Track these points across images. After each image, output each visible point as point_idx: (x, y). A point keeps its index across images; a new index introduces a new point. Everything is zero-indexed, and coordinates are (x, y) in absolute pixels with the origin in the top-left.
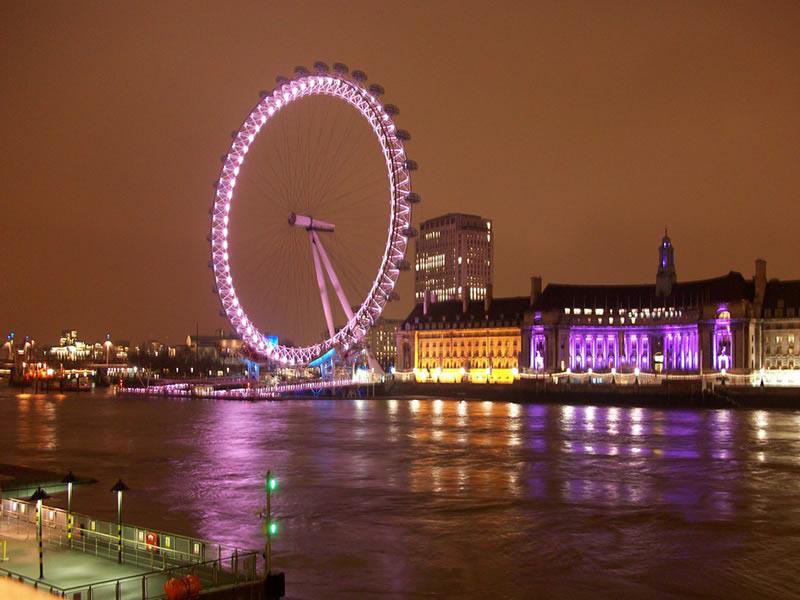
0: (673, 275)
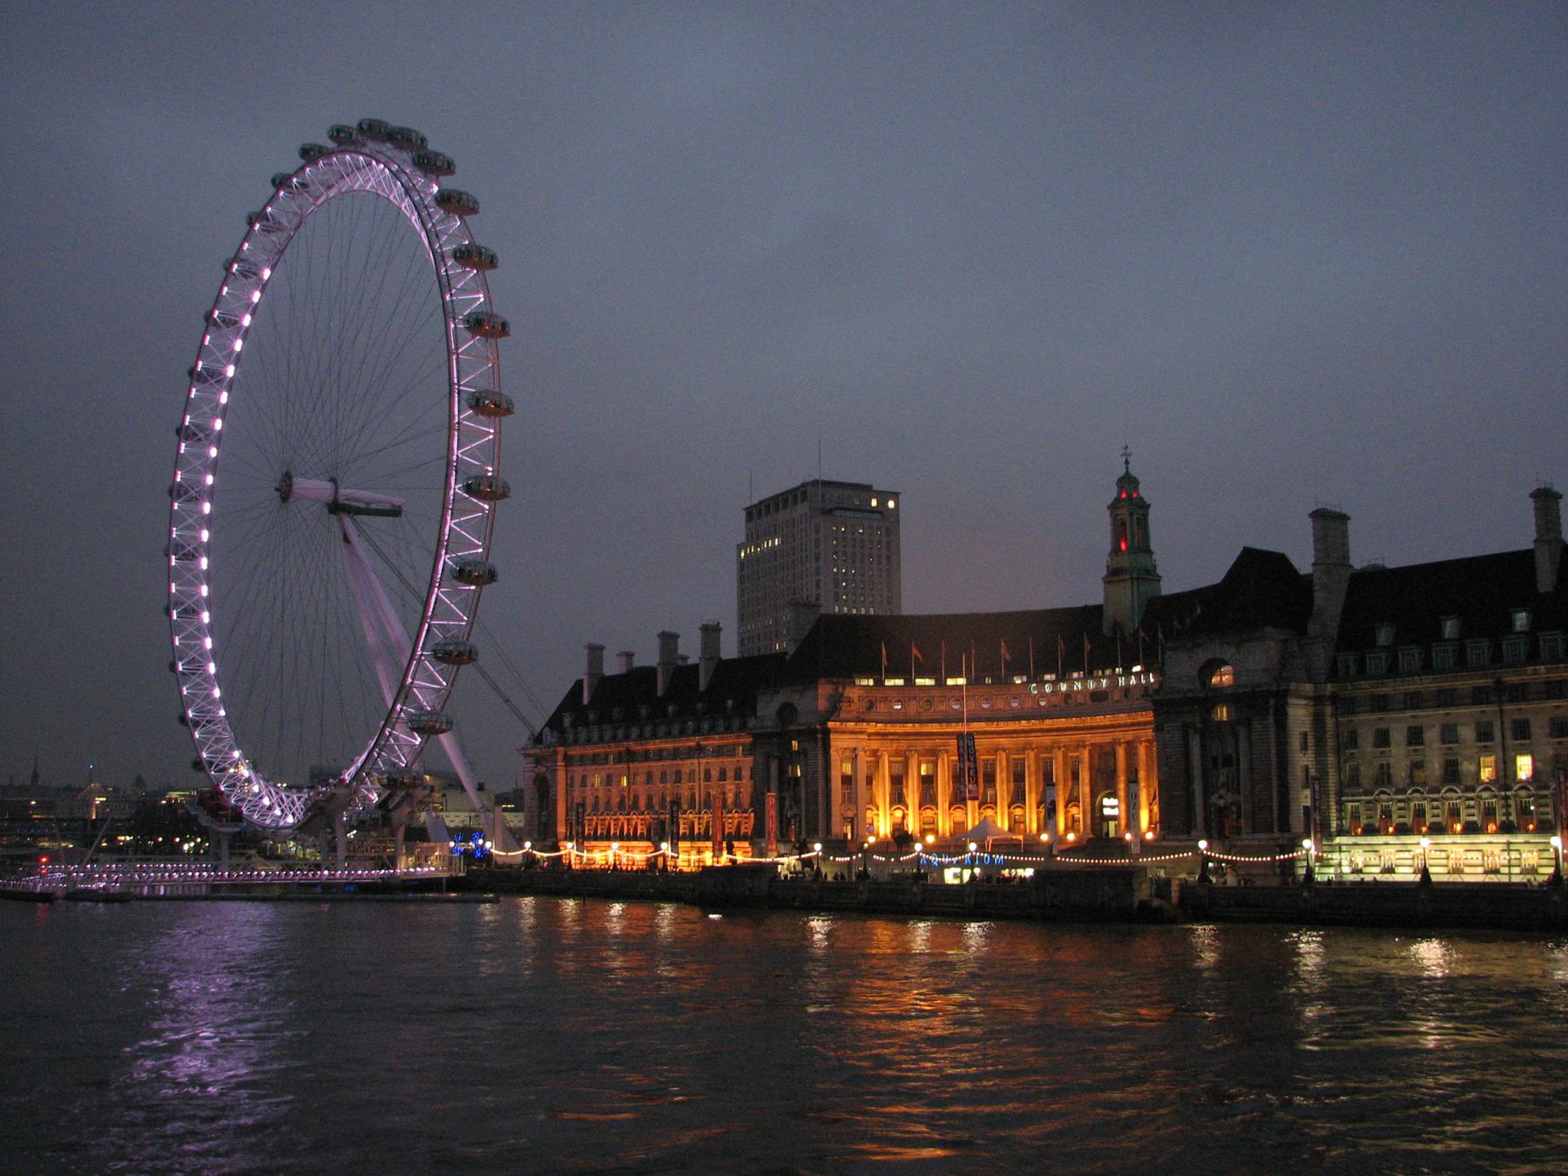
0: (1149, 574)
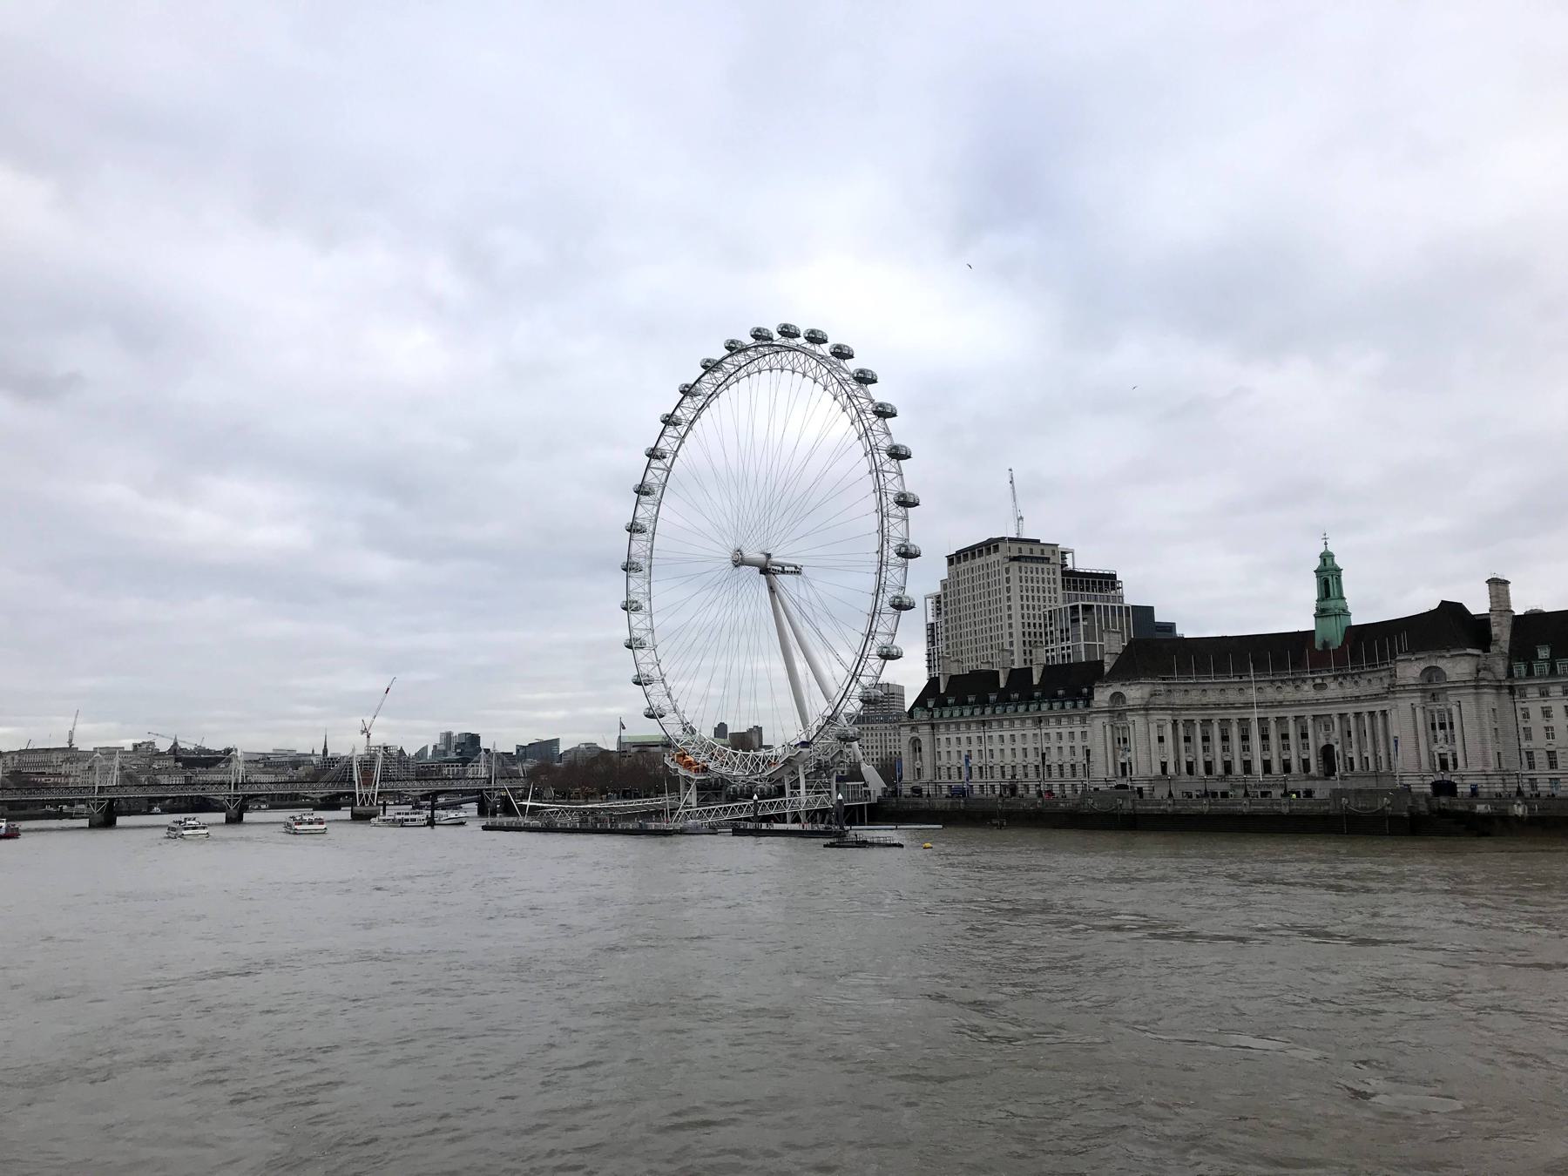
0: (1345, 613)
